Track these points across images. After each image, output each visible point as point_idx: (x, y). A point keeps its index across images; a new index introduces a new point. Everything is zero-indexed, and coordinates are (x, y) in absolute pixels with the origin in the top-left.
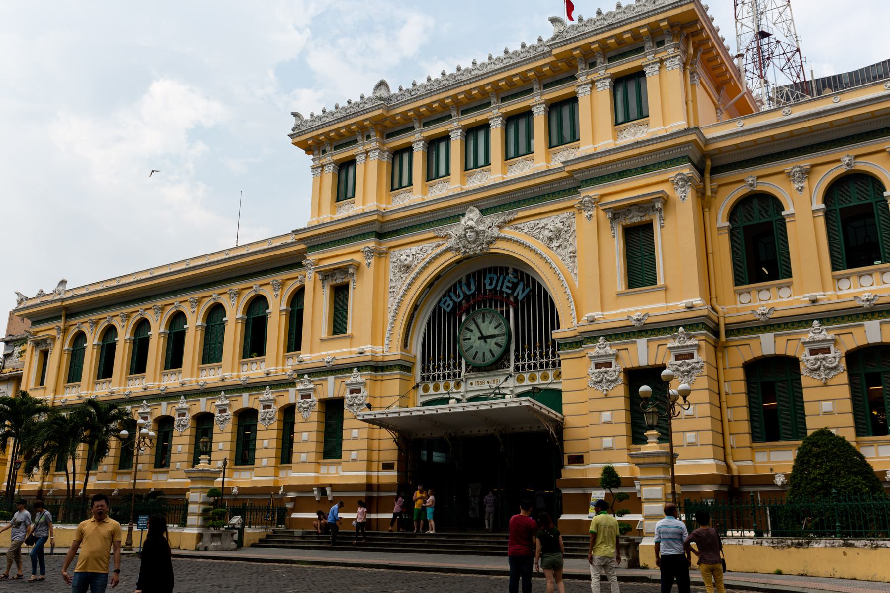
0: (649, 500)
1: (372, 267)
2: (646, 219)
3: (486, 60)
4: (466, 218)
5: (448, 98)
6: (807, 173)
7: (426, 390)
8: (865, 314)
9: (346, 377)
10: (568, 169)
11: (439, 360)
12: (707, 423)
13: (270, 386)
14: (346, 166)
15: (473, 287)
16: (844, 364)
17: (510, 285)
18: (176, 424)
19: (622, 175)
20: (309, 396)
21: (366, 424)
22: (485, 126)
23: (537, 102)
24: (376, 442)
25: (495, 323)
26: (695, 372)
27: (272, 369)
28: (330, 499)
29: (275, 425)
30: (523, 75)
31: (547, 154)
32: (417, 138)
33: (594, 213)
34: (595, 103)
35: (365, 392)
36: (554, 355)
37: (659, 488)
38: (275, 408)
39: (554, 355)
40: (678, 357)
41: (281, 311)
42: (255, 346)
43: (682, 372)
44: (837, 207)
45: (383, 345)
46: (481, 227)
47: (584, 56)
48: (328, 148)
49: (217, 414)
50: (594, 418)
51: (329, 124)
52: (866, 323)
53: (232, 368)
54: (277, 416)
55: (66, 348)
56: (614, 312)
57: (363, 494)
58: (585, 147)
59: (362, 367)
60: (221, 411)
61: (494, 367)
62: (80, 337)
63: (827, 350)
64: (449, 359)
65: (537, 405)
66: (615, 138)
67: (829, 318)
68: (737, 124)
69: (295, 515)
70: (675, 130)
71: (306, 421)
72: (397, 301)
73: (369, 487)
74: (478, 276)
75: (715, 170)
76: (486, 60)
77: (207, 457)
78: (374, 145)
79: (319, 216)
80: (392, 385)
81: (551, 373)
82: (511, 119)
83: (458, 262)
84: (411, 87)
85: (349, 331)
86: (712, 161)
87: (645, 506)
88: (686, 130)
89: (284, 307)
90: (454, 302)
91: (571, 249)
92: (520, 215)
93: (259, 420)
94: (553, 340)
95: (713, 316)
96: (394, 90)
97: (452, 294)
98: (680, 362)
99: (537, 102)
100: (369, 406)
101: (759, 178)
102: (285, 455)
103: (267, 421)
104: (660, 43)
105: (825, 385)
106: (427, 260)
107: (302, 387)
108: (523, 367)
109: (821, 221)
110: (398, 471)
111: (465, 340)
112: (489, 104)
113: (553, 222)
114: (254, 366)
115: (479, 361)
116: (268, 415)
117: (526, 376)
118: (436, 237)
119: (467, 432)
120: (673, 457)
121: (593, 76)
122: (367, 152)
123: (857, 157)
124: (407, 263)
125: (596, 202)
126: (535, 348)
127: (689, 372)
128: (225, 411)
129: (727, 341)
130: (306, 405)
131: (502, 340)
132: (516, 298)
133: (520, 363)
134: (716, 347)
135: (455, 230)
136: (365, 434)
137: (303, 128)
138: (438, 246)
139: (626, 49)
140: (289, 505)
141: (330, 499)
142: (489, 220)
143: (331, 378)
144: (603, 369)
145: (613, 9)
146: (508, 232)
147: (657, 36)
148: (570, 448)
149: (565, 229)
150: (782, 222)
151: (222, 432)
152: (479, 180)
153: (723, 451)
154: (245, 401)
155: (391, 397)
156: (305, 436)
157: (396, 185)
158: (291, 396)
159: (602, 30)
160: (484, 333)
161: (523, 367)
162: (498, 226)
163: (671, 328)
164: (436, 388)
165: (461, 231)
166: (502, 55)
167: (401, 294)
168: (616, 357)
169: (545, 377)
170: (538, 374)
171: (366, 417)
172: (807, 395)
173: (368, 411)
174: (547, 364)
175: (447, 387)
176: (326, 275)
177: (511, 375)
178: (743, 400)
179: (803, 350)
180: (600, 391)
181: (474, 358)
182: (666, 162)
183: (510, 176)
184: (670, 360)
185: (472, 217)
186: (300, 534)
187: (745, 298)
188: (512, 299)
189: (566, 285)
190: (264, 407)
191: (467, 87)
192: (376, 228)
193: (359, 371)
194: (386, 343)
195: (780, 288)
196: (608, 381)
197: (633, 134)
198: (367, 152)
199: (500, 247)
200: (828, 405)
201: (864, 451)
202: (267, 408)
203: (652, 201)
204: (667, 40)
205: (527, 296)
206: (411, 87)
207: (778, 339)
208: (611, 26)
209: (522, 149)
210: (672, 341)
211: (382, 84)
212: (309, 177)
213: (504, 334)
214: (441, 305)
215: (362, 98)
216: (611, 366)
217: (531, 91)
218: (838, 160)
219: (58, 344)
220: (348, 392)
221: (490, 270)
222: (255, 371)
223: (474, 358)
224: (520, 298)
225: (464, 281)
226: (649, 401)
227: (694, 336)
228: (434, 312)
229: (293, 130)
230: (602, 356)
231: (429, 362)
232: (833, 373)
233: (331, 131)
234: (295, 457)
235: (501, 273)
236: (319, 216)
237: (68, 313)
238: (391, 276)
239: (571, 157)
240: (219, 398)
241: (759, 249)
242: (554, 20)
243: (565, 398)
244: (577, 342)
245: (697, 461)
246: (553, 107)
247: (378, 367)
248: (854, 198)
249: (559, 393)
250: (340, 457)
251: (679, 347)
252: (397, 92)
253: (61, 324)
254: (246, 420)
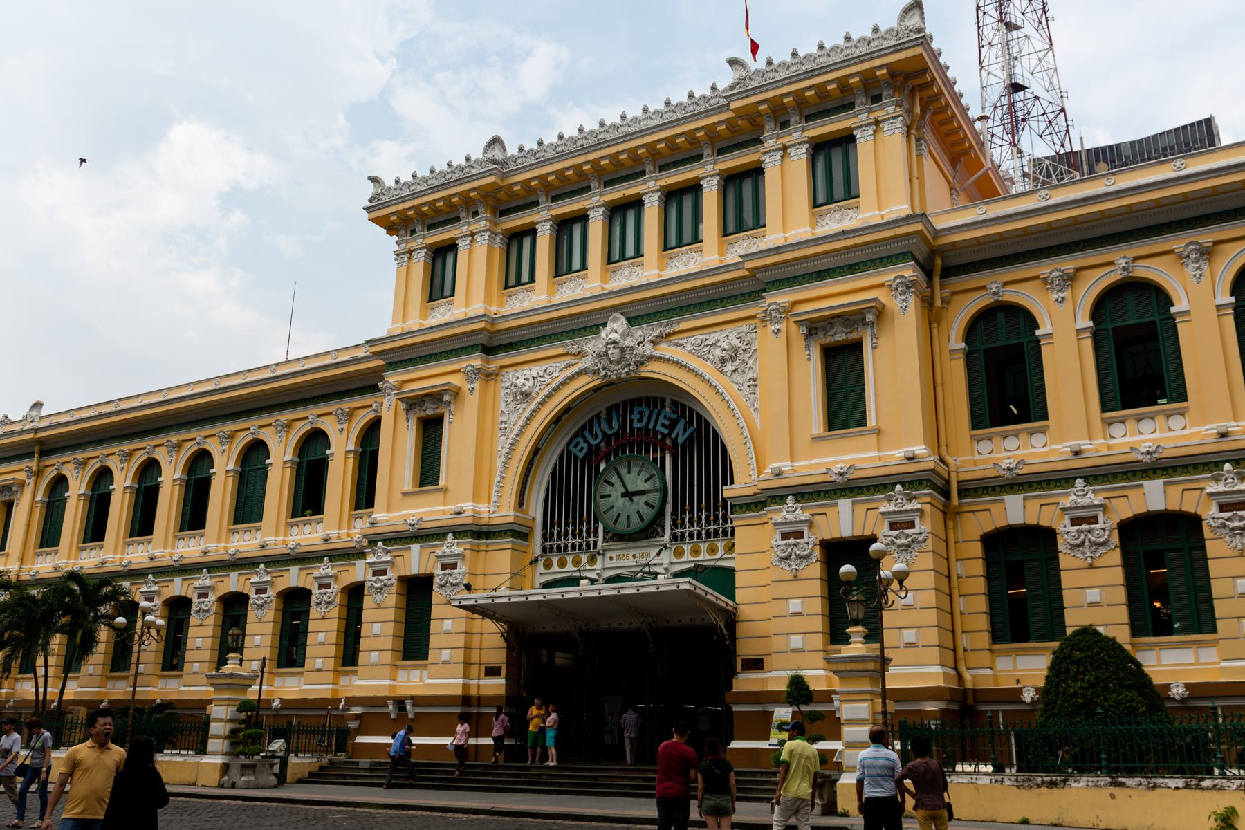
0: (852, 722)
1: (476, 393)
2: (854, 336)
3: (639, 114)
4: (608, 328)
5: (586, 163)
6: (1069, 280)
7: (548, 565)
8: (1144, 471)
9: (437, 546)
10: (749, 265)
11: (567, 525)
12: (931, 617)
13: (330, 557)
14: (443, 253)
15: (615, 424)
16: (1115, 539)
17: (667, 422)
18: (194, 608)
19: (821, 275)
20: (384, 572)
21: (464, 613)
22: (636, 203)
23: (709, 173)
24: (477, 638)
25: (645, 475)
26: (916, 546)
27: (333, 533)
28: (410, 716)
29: (335, 612)
30: (689, 135)
31: (721, 244)
32: (543, 217)
33: (783, 326)
34: (787, 176)
35: (462, 568)
36: (725, 520)
37: (865, 705)
38: (336, 588)
39: (725, 520)
40: (893, 526)
41: (347, 452)
42: (308, 498)
43: (899, 546)
44: (1110, 326)
45: (489, 503)
46: (628, 342)
47: (773, 112)
48: (418, 228)
49: (253, 595)
50: (778, 608)
51: (422, 194)
52: (1146, 483)
53: (276, 531)
54: (338, 600)
55: (39, 498)
56: (808, 463)
57: (458, 710)
58: (772, 237)
59: (460, 533)
60: (258, 592)
61: (643, 535)
62: (60, 482)
63: (1094, 520)
64: (581, 523)
65: (702, 589)
66: (813, 225)
67: (1097, 475)
68: (977, 210)
69: (360, 739)
70: (894, 217)
71: (379, 607)
72: (510, 441)
73: (466, 700)
74: (623, 409)
75: (947, 272)
76: (639, 114)
77: (238, 655)
78: (483, 224)
79: (404, 321)
80: (501, 558)
81: (720, 545)
82: (672, 195)
83: (596, 389)
84: (535, 147)
85: (442, 482)
86: (942, 259)
87: (846, 729)
88: (909, 217)
89: (351, 447)
90: (589, 443)
91: (750, 375)
92: (683, 326)
93: (312, 604)
94: (724, 500)
95: (942, 470)
96: (512, 150)
97: (586, 433)
98: (897, 532)
99: (709, 173)
100: (468, 587)
101: (1006, 284)
102: (349, 654)
103: (323, 606)
104: (876, 99)
105: (1091, 566)
106: (553, 385)
107: (374, 559)
108: (683, 535)
109: (1088, 345)
110: (507, 679)
111: (603, 497)
112: (643, 173)
113: (727, 338)
114: (308, 529)
115: (621, 527)
116: (325, 598)
117: (687, 548)
118: (567, 354)
119: (603, 625)
120: (884, 662)
121: (785, 140)
122: (473, 235)
123: (1136, 259)
124: (525, 389)
125: (786, 311)
126: (699, 510)
127: (908, 546)
128: (264, 591)
129: (960, 505)
130: (379, 585)
131: (654, 498)
132: (675, 441)
133: (679, 530)
134: (945, 513)
135: (593, 345)
136: (462, 626)
137: (385, 199)
138: (568, 366)
139: (830, 105)
140: (353, 725)
141: (410, 716)
142: (640, 332)
143: (415, 548)
144: (792, 541)
145: (814, 50)
146: (665, 350)
147: (873, 88)
148: (746, 649)
149: (744, 347)
150: (1036, 344)
151: (260, 621)
152: (628, 277)
153: (953, 654)
154: (294, 577)
155: (500, 575)
156: (377, 628)
157: (512, 281)
158: (358, 571)
159: (798, 78)
160: (630, 488)
161: (683, 535)
162: (652, 341)
163: (885, 486)
164: (562, 564)
165: (600, 347)
166: (662, 107)
167: (516, 432)
168: (810, 524)
169: (713, 550)
170: (704, 547)
171: (464, 603)
172: (1067, 579)
173: (466, 595)
174: (716, 532)
175: (577, 562)
176: (413, 403)
177: (666, 547)
178: (980, 585)
179: (1062, 517)
180: (787, 570)
181: (615, 523)
182: (881, 259)
183: (669, 273)
184: (884, 530)
185: (616, 328)
186: (367, 766)
187: (985, 447)
188: (669, 442)
189: (743, 424)
190: (321, 586)
191: (613, 150)
192: (483, 339)
193: (455, 538)
194: (493, 499)
195: (1032, 434)
196: (798, 557)
197: (837, 221)
198: (473, 235)
199: (654, 370)
200: (1094, 594)
201: (1141, 657)
202: (325, 587)
203: (862, 312)
204: (885, 94)
205: (690, 438)
206: (535, 147)
207: (1029, 503)
208: (811, 73)
209: (687, 236)
210: (886, 503)
211: (496, 141)
212: (390, 267)
213: (657, 490)
214: (571, 448)
215: (468, 159)
216: (802, 537)
217: (700, 157)
218: (1112, 263)
219: (28, 492)
220: (439, 566)
221: (640, 401)
222: (308, 535)
223: (615, 523)
224: (680, 440)
225: (603, 416)
226: (853, 586)
227: (915, 497)
228: (561, 457)
229: (370, 201)
230: (791, 523)
231: (552, 526)
232: (1101, 550)
233: (423, 204)
234: (362, 658)
235: (655, 406)
236: (404, 321)
237: (44, 448)
238: (503, 407)
239: (753, 250)
240: (257, 573)
241: (1005, 382)
242: (733, 63)
243: (740, 580)
244: (757, 503)
245: (917, 668)
246: (731, 180)
247: (481, 533)
248: (1132, 315)
249: (730, 572)
250: (426, 657)
251: (895, 512)
252: (516, 152)
253: (33, 464)
254: (295, 604)
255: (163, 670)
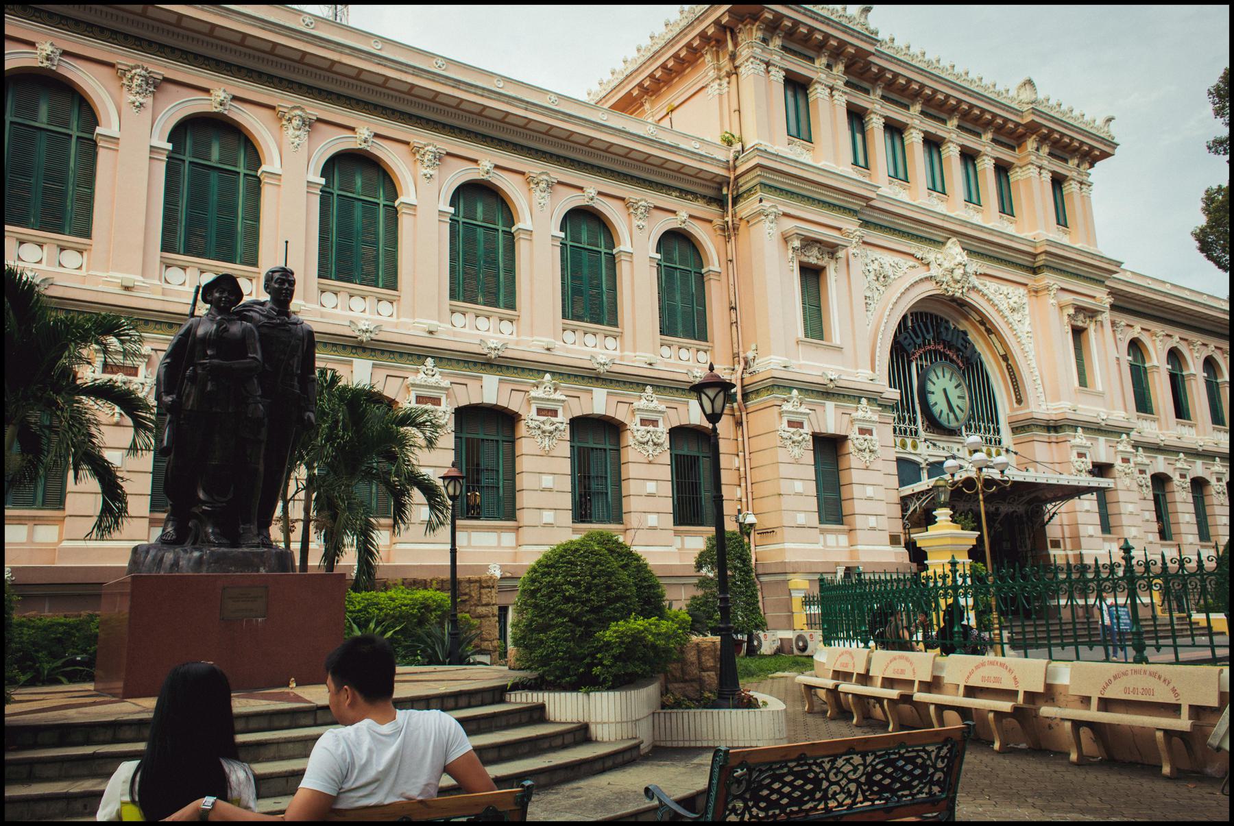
46: (970, 270)
135: (931, 254)
185: (954, 252)
199: (974, 299)
255: (821, 522)
